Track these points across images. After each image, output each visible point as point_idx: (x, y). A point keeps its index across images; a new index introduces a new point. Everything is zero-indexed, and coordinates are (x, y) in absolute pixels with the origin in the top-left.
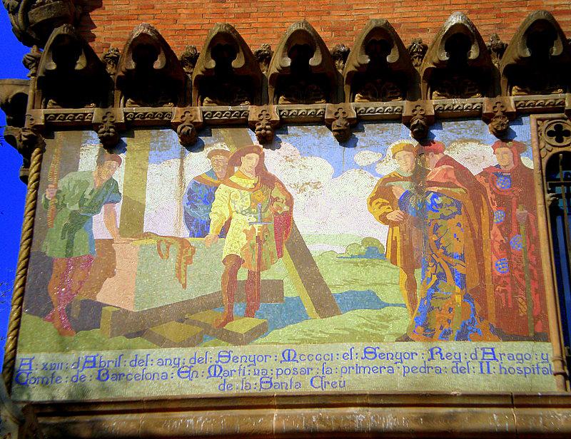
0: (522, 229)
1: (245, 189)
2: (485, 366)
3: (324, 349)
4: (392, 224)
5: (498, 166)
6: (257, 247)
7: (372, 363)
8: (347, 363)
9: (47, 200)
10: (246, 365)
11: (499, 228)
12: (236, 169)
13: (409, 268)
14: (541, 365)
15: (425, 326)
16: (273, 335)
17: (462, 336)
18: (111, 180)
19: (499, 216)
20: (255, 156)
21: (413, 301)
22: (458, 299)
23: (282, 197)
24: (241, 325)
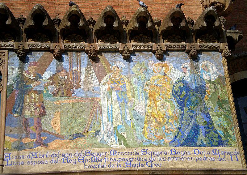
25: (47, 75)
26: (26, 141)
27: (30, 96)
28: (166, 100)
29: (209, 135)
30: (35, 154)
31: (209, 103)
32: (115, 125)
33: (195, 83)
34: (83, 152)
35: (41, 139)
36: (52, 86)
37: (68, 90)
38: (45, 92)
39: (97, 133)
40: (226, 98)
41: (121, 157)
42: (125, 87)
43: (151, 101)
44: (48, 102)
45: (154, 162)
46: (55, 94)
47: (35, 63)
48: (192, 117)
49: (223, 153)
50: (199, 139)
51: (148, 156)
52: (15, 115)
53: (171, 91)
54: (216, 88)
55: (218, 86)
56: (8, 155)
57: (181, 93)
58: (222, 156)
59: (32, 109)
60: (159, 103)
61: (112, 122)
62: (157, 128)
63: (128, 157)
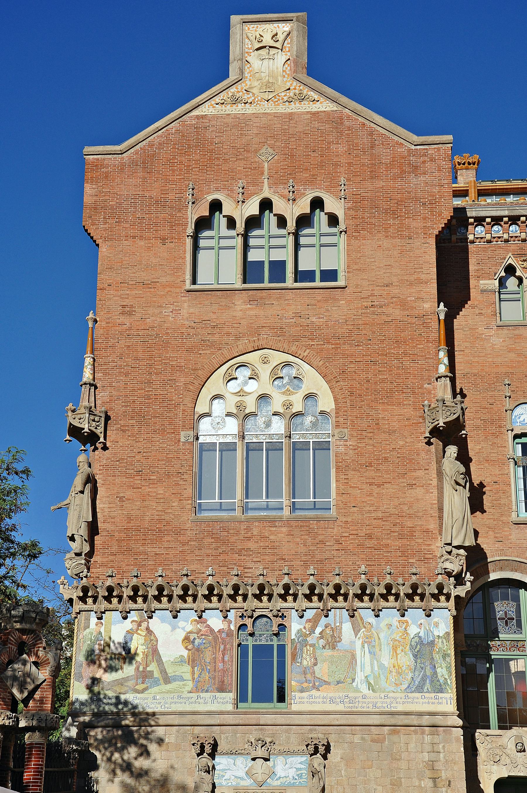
0: (229, 652)
1: (142, 636)
2: (213, 701)
3: (166, 695)
4: (189, 650)
5: (223, 629)
6: (146, 659)
7: (179, 701)
8: (172, 701)
9: (80, 639)
10: (142, 701)
11: (222, 652)
12: (140, 628)
13: (193, 668)
14: (229, 701)
15: (197, 687)
16: (149, 691)
17: (207, 691)
18: (100, 632)
19: (222, 647)
20: (146, 623)
21: (193, 679)
22: (207, 678)
23: (154, 639)
24: (140, 687)
25: (318, 630)
26: (305, 685)
27: (307, 648)
28: (405, 652)
29: (433, 684)
30: (311, 696)
31: (437, 657)
32: (366, 675)
33: (428, 637)
34: (344, 696)
35: (315, 685)
36: (322, 640)
37: (333, 645)
38: (317, 645)
39: (353, 680)
40: (449, 652)
41: (369, 700)
42: (374, 641)
43: (393, 654)
44: (318, 652)
45: (392, 705)
46: (324, 647)
47: (309, 621)
48: (422, 668)
49: (441, 698)
50: (426, 688)
51: (388, 701)
52: (297, 664)
53: (409, 645)
54: (442, 642)
55: (445, 641)
56: (294, 696)
57: (416, 648)
58: (440, 701)
59: (308, 659)
60: (399, 656)
61: (364, 673)
62: (396, 678)
63: (374, 700)
